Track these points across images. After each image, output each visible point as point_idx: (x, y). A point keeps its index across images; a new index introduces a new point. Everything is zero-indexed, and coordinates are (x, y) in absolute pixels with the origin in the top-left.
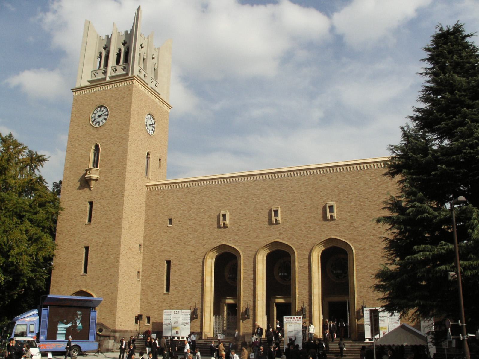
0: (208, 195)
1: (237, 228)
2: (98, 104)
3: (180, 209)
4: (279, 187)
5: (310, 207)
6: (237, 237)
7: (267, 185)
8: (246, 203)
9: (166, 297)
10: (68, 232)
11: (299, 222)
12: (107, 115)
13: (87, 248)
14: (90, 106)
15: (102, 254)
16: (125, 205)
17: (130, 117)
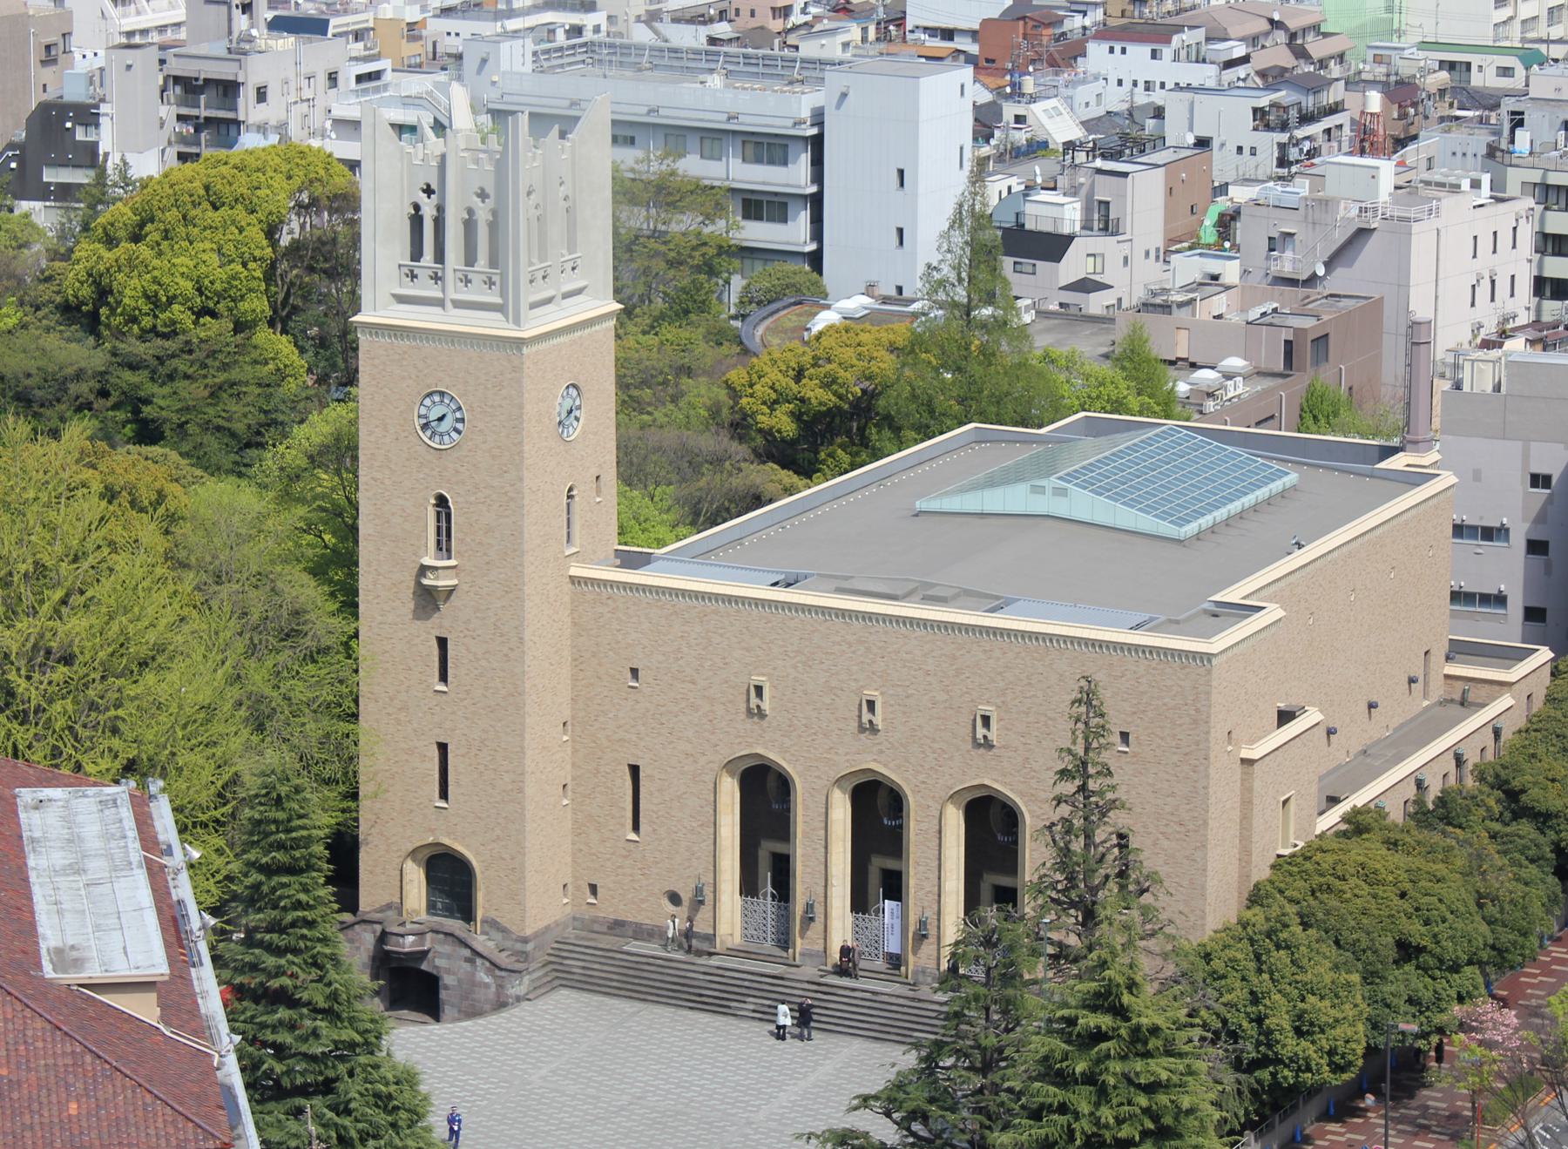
9: (632, 845)
12: (462, 420)
15: (482, 768)
17: (521, 443)
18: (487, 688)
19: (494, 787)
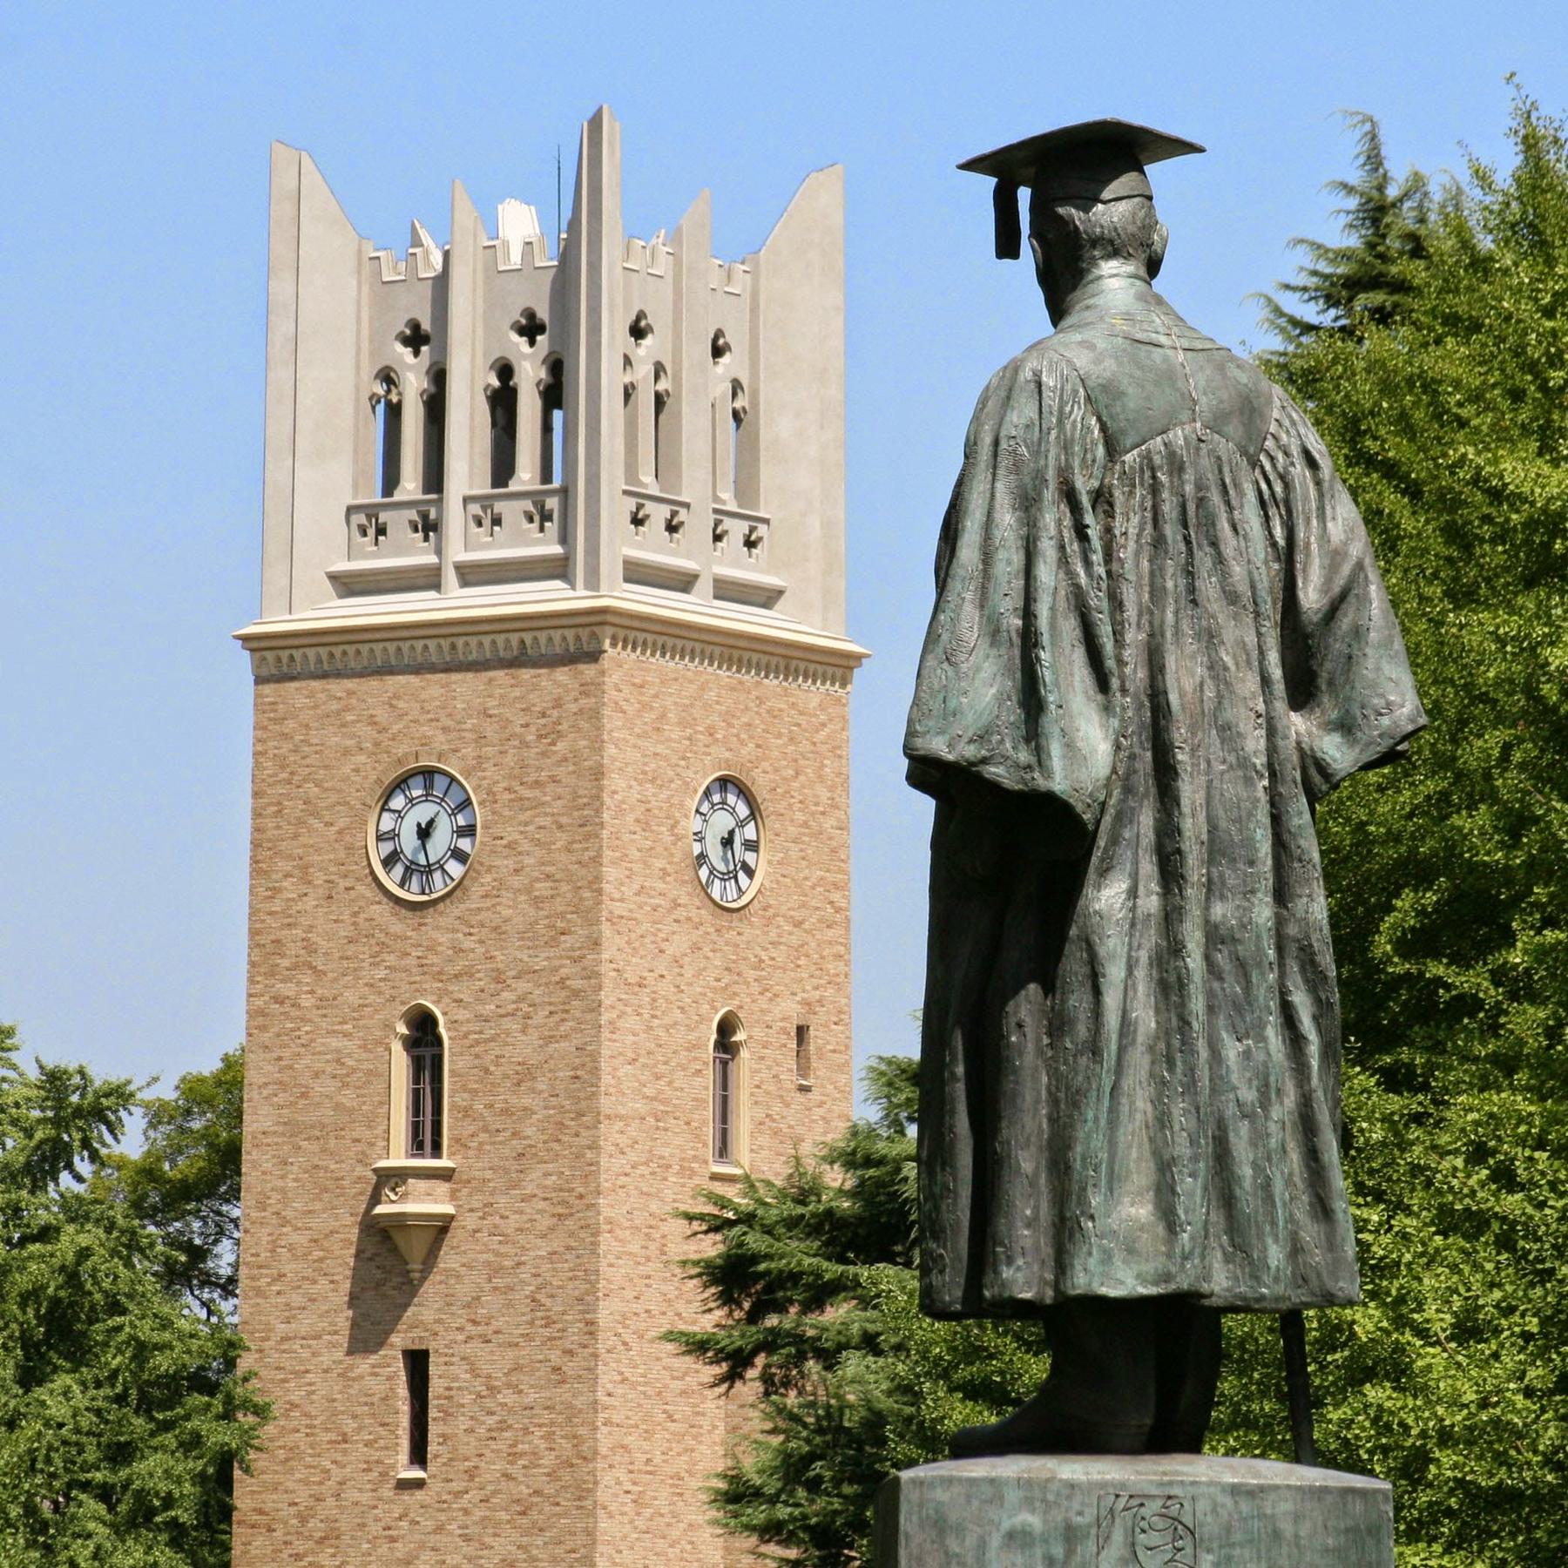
10: (303, 1520)
14: (362, 758)
16: (607, 1377)
17: (597, 860)
18: (513, 1456)
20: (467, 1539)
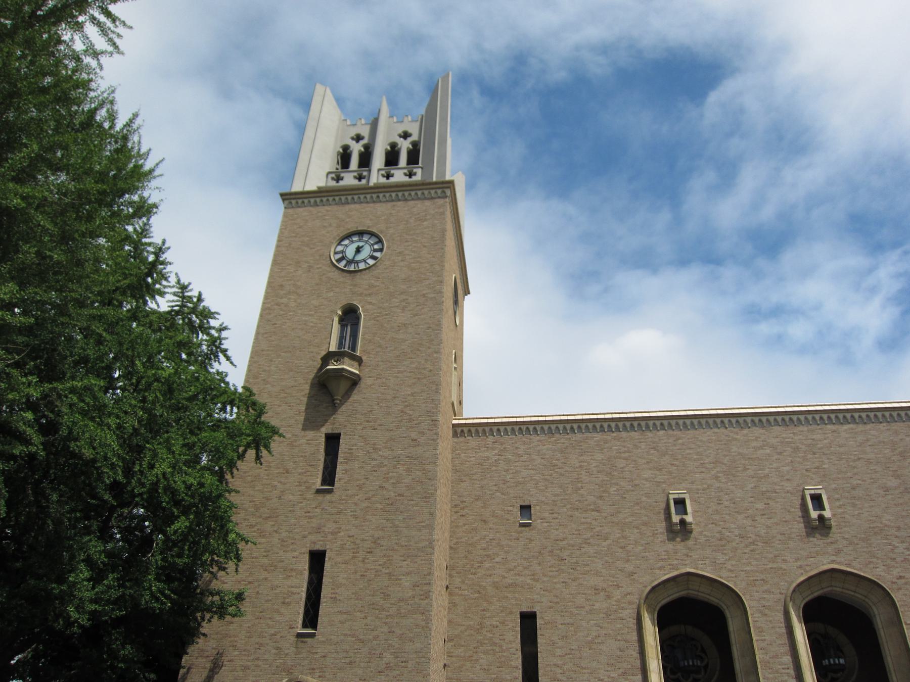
0: (623, 455)
1: (718, 535)
2: (352, 227)
3: (552, 483)
4: (809, 446)
5: (897, 491)
6: (721, 558)
7: (778, 440)
8: (731, 478)
10: (257, 509)
11: (879, 525)
13: (317, 559)
19: (386, 596)
20: (356, 517)
